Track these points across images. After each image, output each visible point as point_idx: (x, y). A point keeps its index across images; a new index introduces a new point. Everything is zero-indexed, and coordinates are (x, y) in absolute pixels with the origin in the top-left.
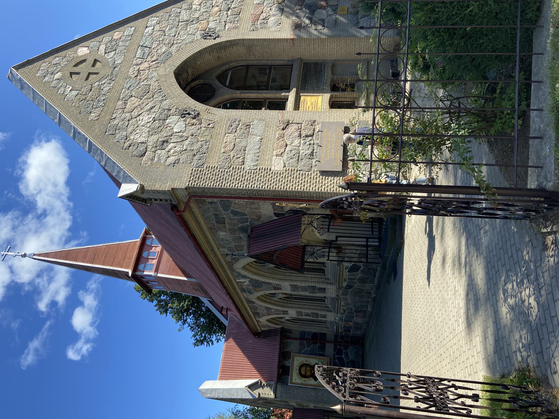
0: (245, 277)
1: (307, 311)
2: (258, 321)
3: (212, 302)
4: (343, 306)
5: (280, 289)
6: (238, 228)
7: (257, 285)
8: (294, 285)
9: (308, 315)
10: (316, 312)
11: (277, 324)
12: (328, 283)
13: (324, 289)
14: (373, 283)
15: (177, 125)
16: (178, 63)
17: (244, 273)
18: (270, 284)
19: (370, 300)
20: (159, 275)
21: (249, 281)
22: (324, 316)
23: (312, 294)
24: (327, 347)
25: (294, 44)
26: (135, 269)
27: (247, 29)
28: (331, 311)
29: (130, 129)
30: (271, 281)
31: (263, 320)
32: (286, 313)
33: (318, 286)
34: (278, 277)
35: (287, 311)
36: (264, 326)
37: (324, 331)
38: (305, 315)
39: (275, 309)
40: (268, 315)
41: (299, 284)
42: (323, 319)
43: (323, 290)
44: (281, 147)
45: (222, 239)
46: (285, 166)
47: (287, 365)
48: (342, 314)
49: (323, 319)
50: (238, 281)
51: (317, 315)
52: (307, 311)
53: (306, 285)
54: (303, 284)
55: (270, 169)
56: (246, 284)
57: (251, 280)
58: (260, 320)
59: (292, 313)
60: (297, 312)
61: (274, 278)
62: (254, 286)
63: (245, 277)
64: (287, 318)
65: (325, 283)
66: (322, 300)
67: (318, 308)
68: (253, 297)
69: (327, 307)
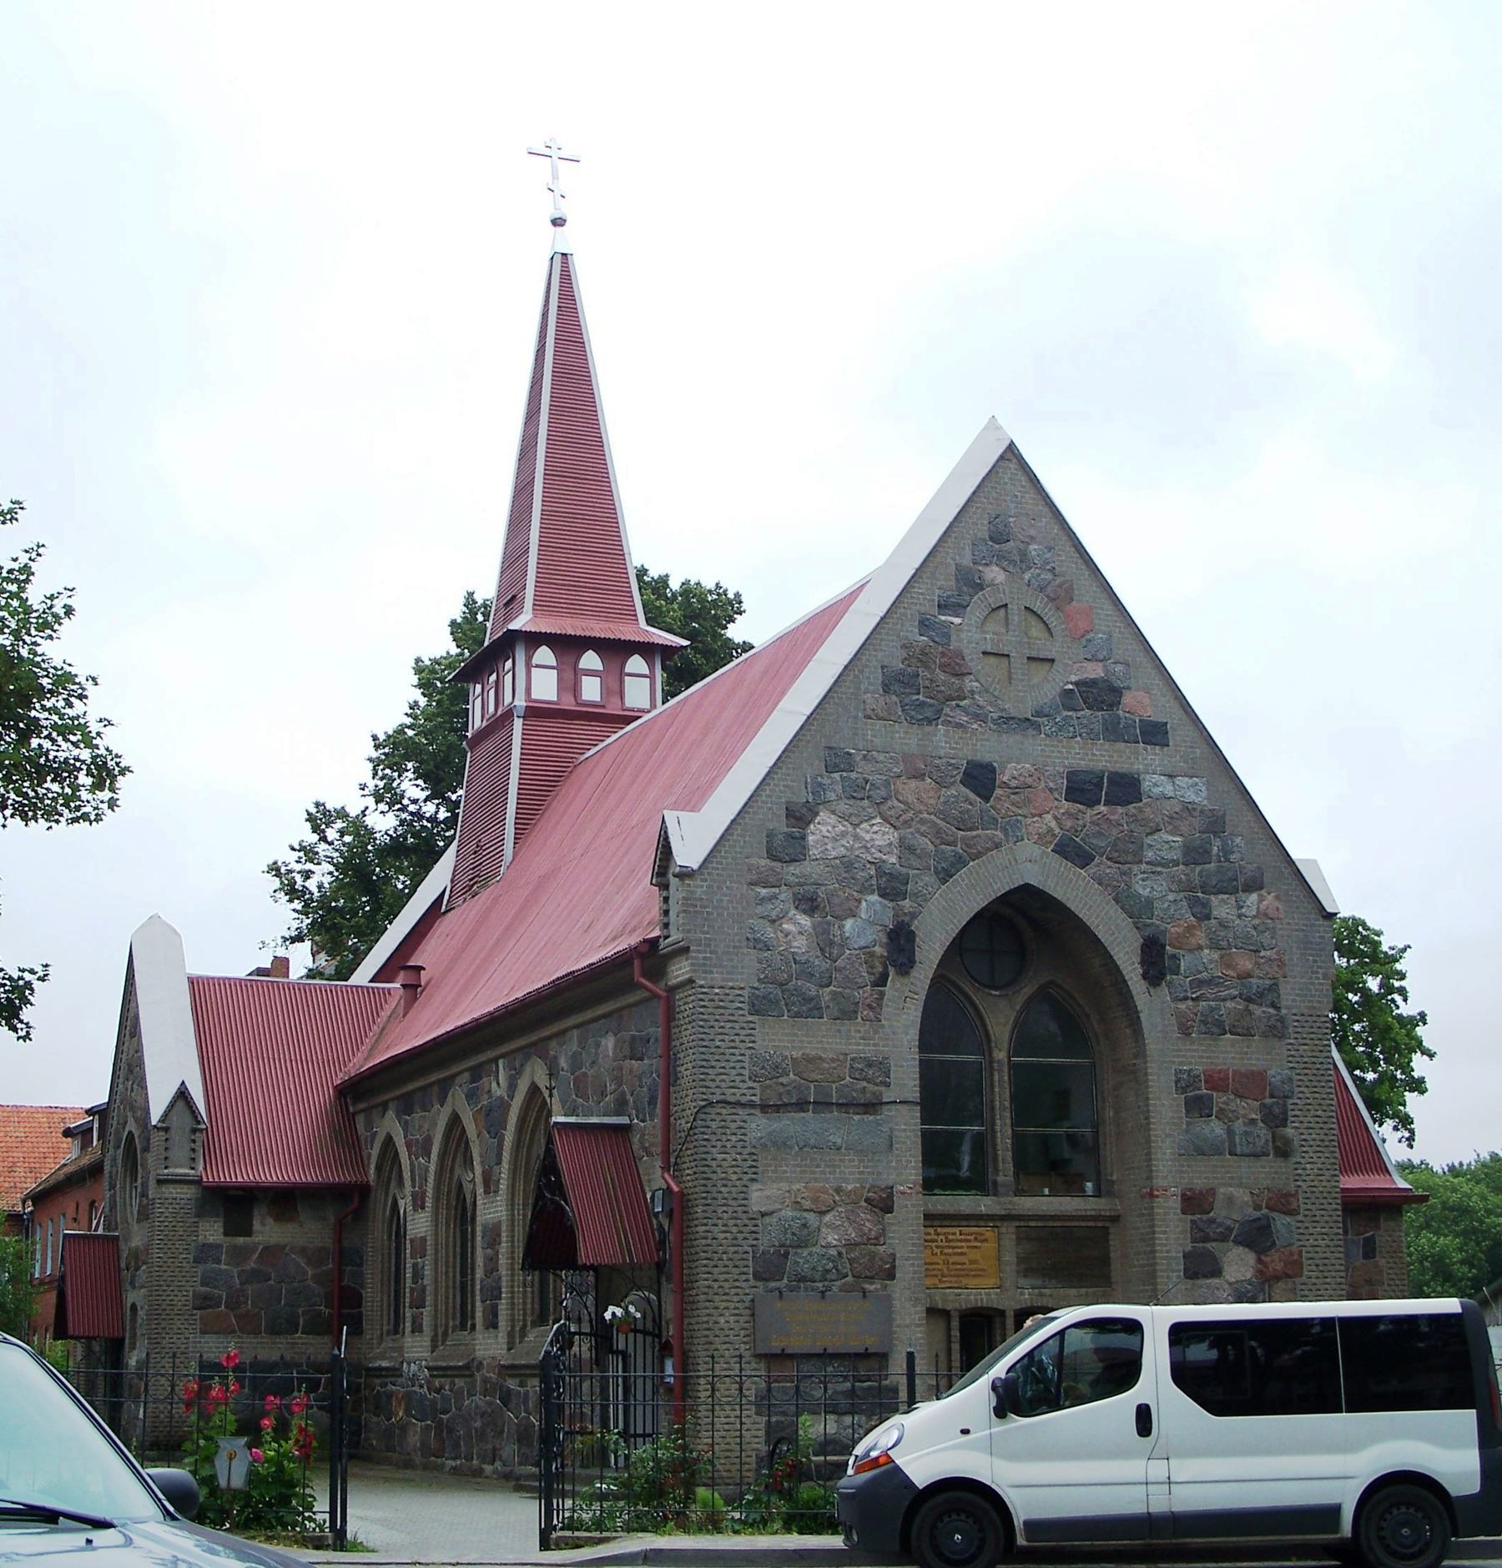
0: (512, 1087)
1: (428, 1271)
2: (384, 1106)
3: (434, 912)
4: (453, 1383)
5: (487, 1192)
6: (623, 1094)
7: (493, 1118)
8: (499, 1235)
9: (417, 1274)
10: (429, 1299)
11: (379, 1168)
12: (511, 1335)
13: (495, 1326)
14: (520, 1464)
15: (864, 926)
16: (1058, 893)
18: (499, 1163)
19: (475, 1462)
20: (518, 724)
21: (501, 1098)
22: (417, 1328)
23: (478, 1287)
24: (319, 1339)
25: (1143, 1197)
26: (534, 640)
27: (1181, 1063)
28: (434, 1347)
29: (842, 807)
30: (505, 1165)
33: (503, 1305)
34: (520, 1186)
35: (423, 1208)
36: (369, 1125)
37: (371, 1330)
38: (415, 1266)
39: (427, 1170)
40: (409, 1145)
41: (504, 1247)
42: (408, 1325)
43: (492, 1324)
44: (815, 1200)
45: (598, 1045)
46: (763, 1215)
47: (256, 1212)
48: (428, 1382)
49: (408, 1325)
50: (501, 1062)
51: (419, 1304)
52: (428, 1271)
53: (504, 1271)
54: (503, 1261)
55: (753, 1180)
56: (494, 1085)
57: (504, 1106)
58: (391, 1113)
59: (419, 1224)
60: (424, 1240)
61: (514, 1172)
62: (489, 1112)
63: (512, 1087)
64: (401, 1203)
65: (513, 1327)
66: (465, 1320)
67: (442, 1308)
68: (457, 1099)
69: (445, 1334)
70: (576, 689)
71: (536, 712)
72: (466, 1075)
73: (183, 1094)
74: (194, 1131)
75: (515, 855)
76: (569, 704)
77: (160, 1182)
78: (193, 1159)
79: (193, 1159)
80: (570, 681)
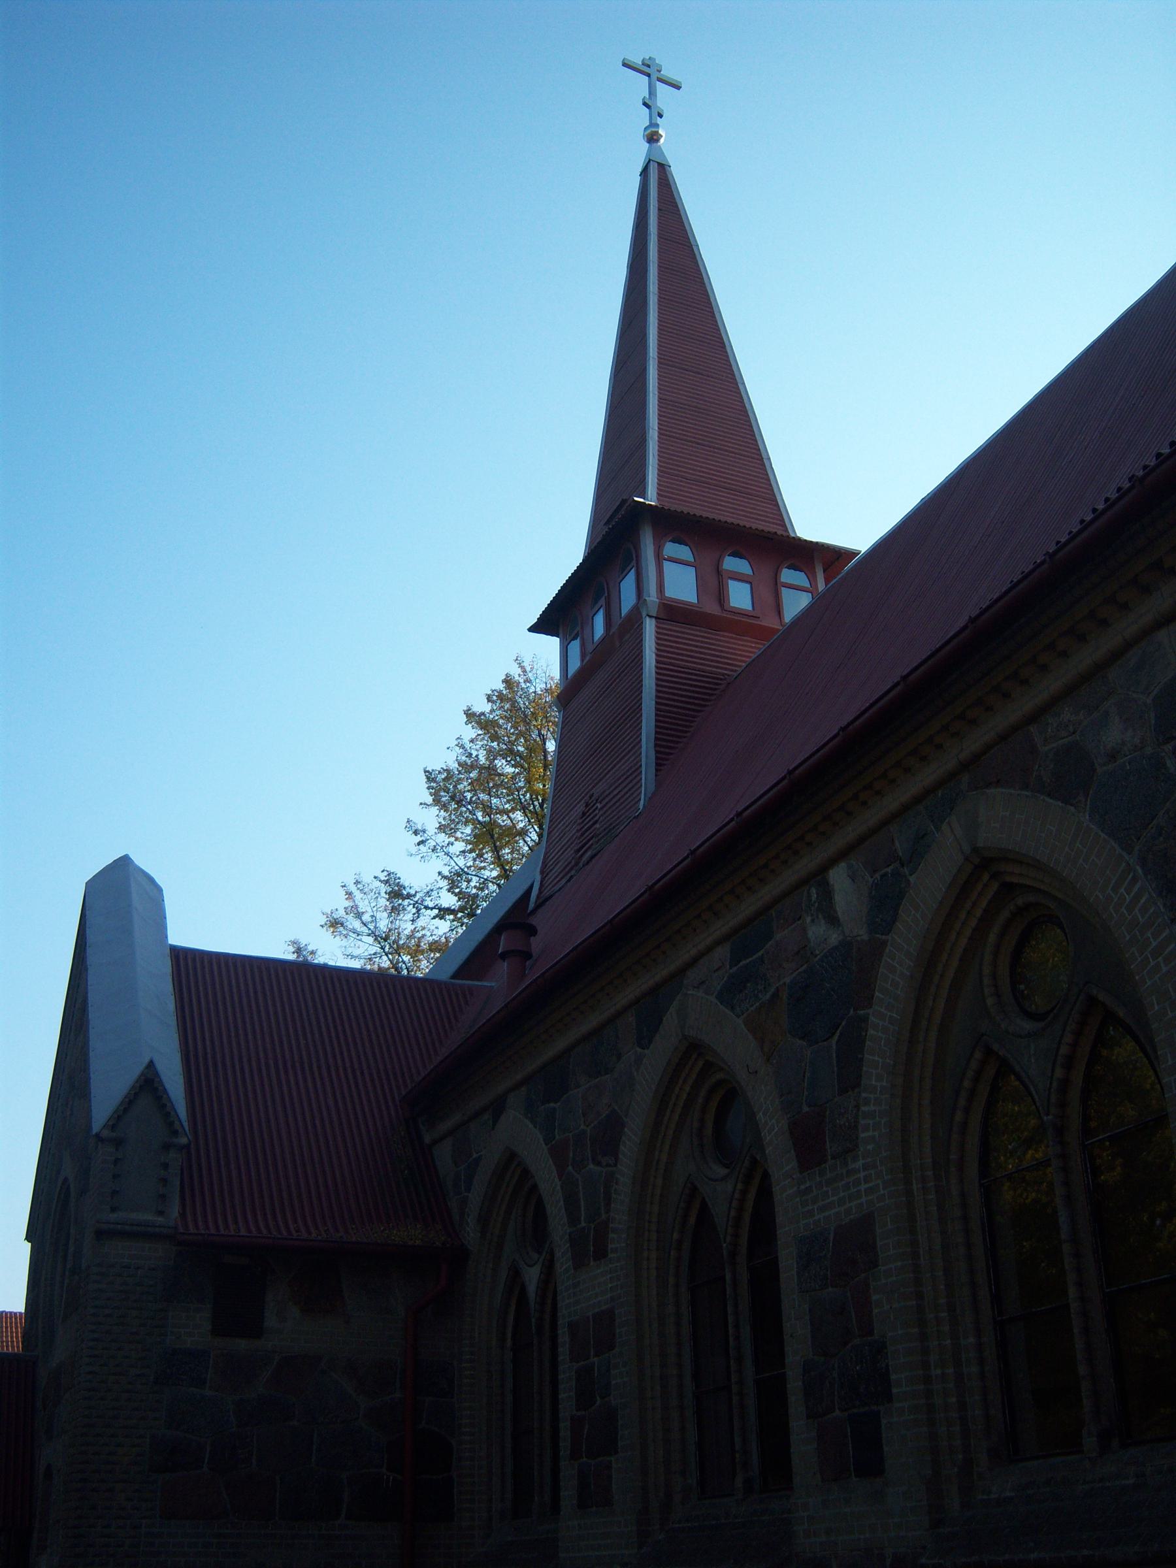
0: (885, 903)
2: (498, 1108)
17: (930, 884)
20: (650, 628)
26: (672, 524)
31: (519, 1133)
32: (591, 1247)
35: (601, 1254)
42: (569, 1495)
43: (859, 1454)
49: (569, 1495)
50: (838, 877)
63: (885, 903)
70: (721, 596)
71: (672, 613)
72: (722, 953)
73: (149, 1083)
74: (167, 1147)
75: (659, 784)
76: (712, 608)
77: (100, 1234)
78: (163, 1197)
79: (163, 1197)
80: (714, 584)
